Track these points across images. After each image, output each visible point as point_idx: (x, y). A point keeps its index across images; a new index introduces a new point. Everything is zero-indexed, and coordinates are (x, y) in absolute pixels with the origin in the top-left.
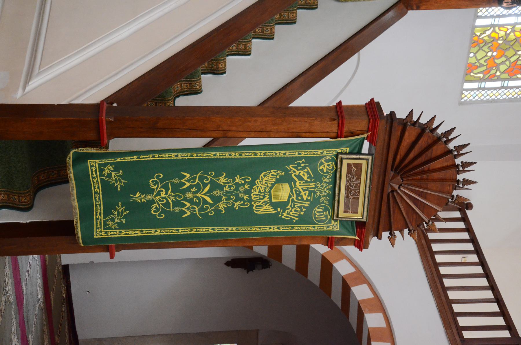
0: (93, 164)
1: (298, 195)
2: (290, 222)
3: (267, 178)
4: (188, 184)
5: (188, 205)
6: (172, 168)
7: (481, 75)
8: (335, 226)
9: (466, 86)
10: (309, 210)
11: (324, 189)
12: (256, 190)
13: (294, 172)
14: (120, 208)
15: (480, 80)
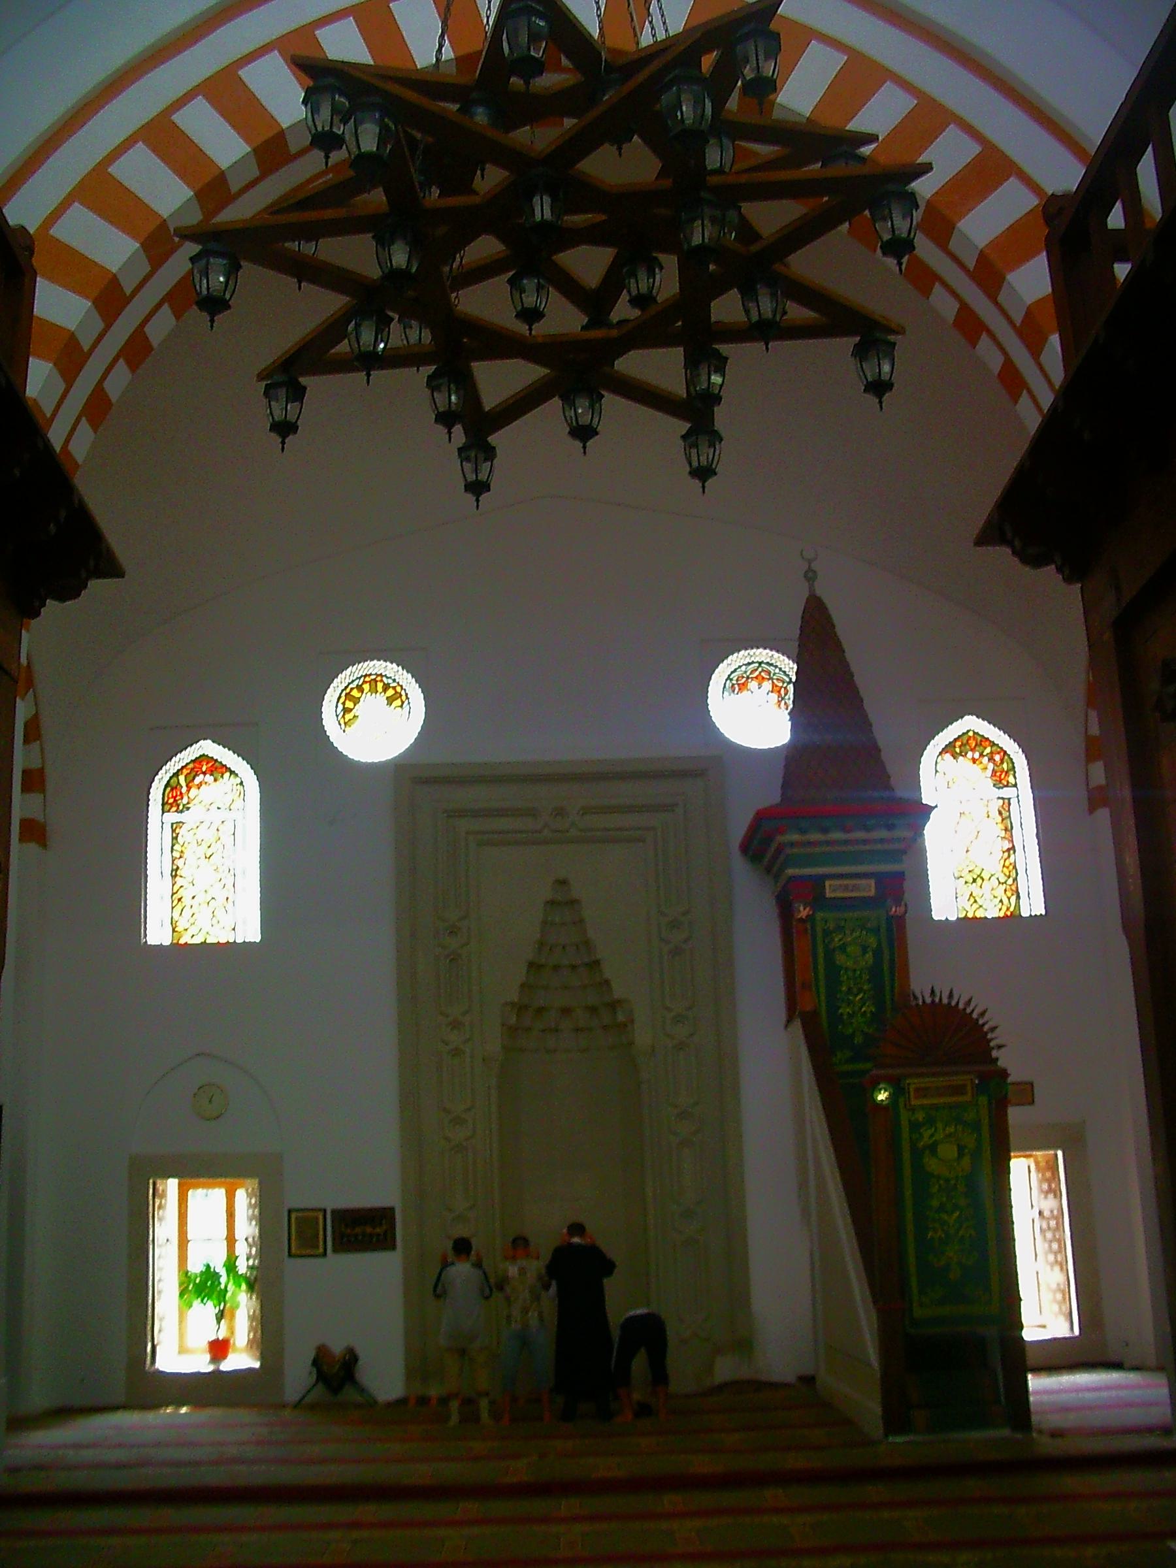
0: (918, 1312)
1: (950, 1135)
3: (932, 1164)
4: (940, 1233)
5: (961, 1233)
8: (983, 1100)
15: (1018, 897)
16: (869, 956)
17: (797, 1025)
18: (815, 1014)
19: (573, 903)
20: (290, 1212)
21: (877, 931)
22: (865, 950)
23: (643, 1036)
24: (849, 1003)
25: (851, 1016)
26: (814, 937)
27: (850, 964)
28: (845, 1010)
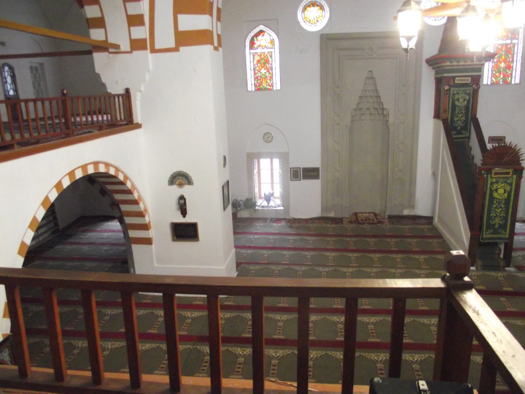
0: (485, 236)
2: (511, 189)
3: (495, 195)
6: (489, 218)
7: (510, 78)
9: (513, 83)
10: (508, 183)
11: (502, 180)
12: (499, 197)
13: (495, 188)
14: (499, 231)
16: (466, 103)
17: (440, 123)
18: (447, 119)
19: (373, 78)
20: (291, 168)
21: (469, 94)
22: (464, 100)
23: (391, 120)
24: (457, 117)
25: (457, 121)
26: (449, 97)
27: (459, 105)
28: (456, 119)
